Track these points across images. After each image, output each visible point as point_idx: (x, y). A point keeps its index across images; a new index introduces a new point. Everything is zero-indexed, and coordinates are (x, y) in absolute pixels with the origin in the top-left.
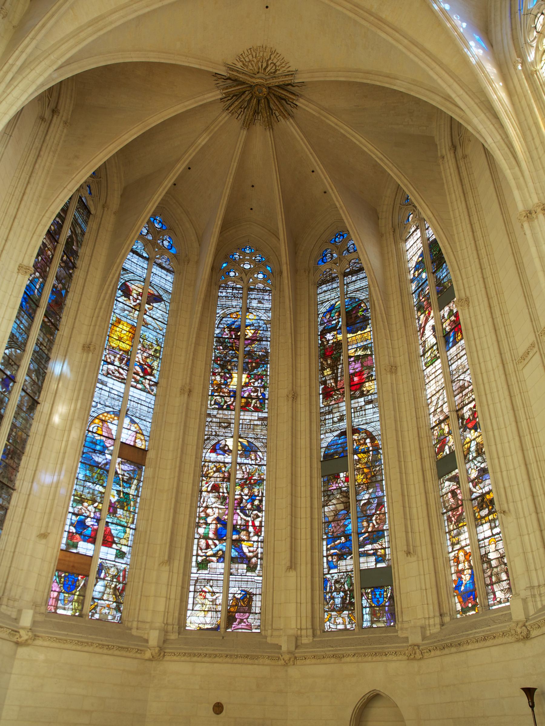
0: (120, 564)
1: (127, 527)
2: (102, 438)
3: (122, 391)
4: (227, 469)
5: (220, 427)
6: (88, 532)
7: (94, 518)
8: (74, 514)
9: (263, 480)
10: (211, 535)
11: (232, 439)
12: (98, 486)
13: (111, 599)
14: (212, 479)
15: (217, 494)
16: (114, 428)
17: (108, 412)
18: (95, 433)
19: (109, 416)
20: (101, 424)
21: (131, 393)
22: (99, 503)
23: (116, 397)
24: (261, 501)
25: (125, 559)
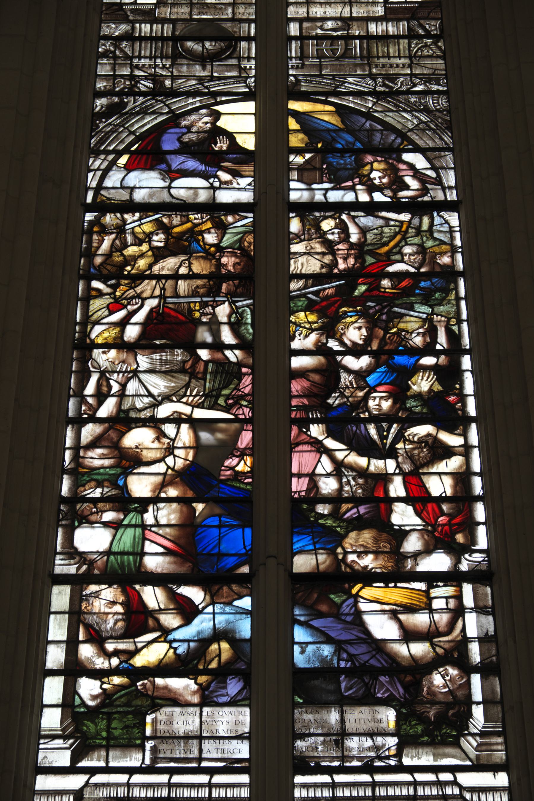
4: (228, 240)
5: (175, 57)
9: (450, 274)
10: (154, 563)
11: (250, 106)
14: (146, 287)
15: (179, 355)
24: (449, 375)
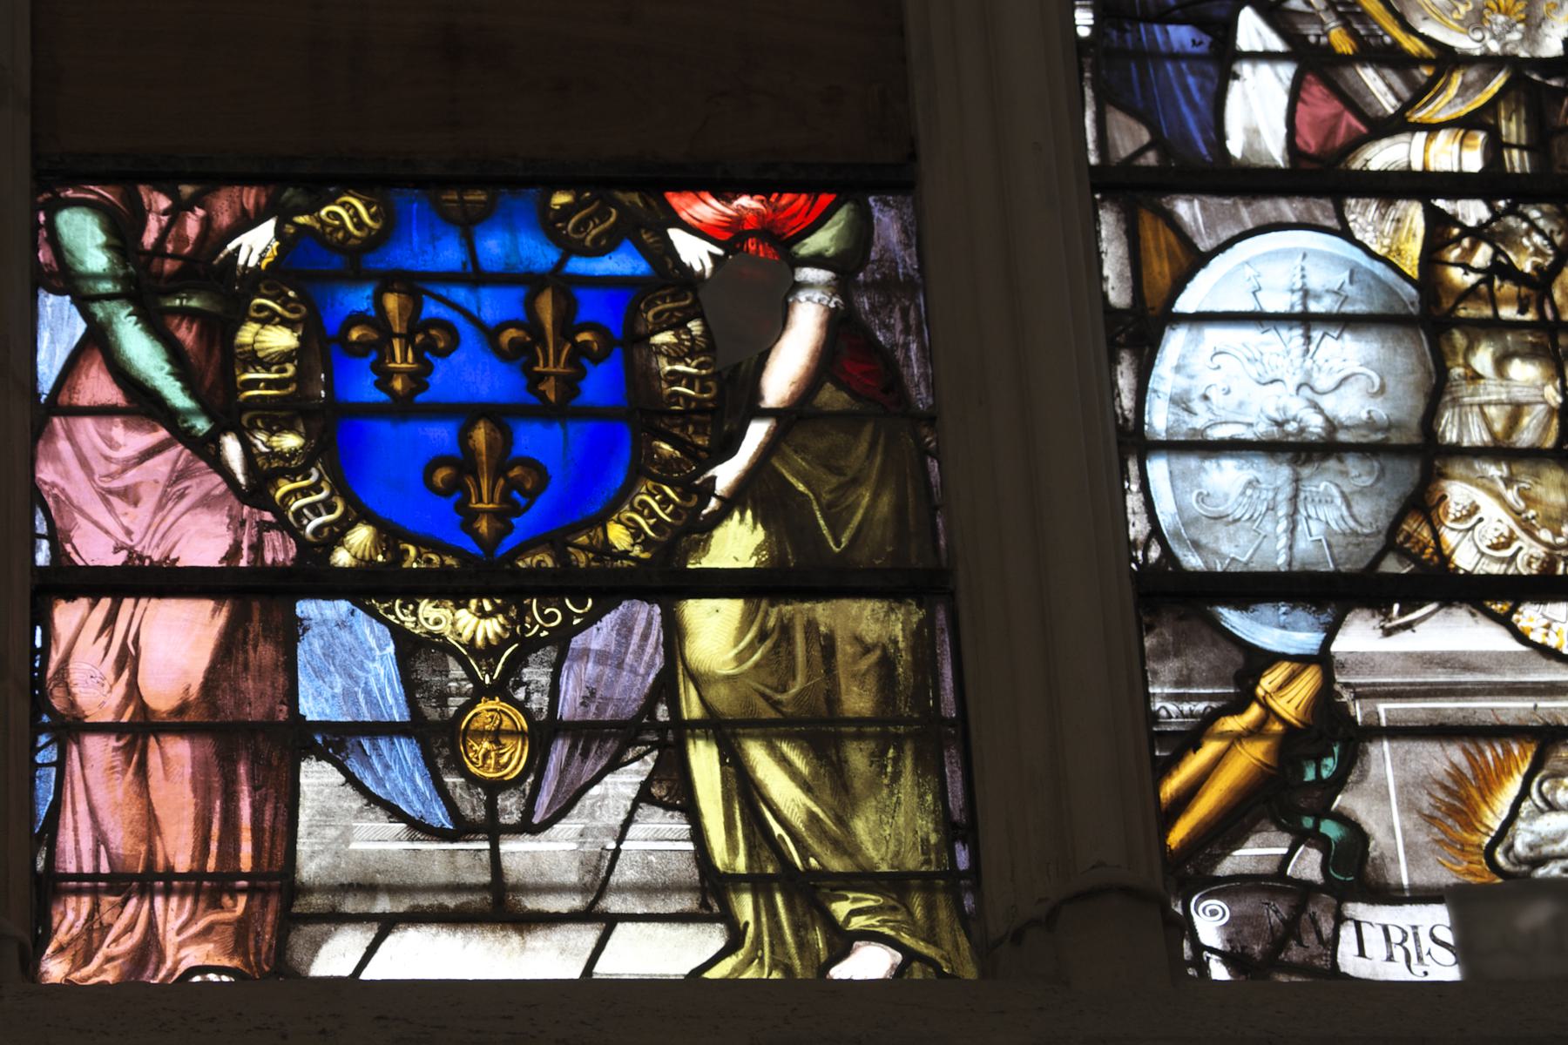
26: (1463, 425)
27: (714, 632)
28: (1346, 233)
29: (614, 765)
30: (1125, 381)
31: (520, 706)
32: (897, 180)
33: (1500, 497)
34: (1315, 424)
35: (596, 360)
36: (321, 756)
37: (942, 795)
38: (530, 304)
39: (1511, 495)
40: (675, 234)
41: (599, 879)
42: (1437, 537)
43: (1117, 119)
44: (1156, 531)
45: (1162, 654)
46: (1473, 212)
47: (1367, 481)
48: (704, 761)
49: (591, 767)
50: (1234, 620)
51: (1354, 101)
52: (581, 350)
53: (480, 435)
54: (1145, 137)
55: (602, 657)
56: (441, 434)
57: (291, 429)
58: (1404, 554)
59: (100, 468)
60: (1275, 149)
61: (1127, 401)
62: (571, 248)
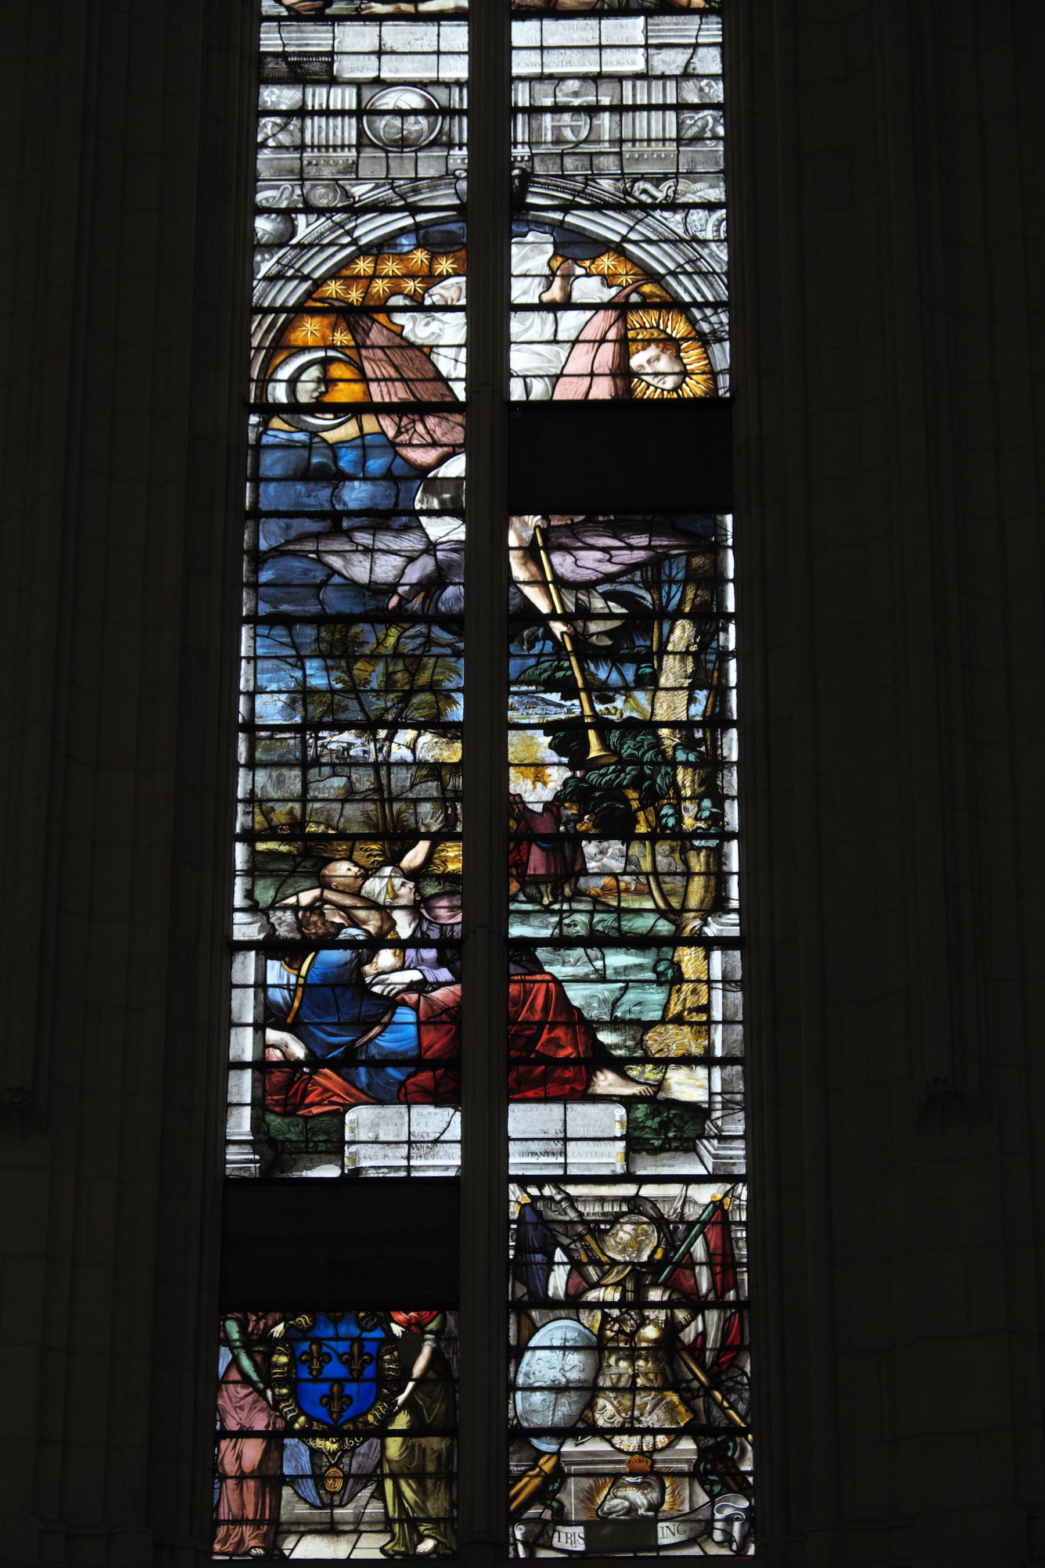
0: (674, 1190)
1: (677, 941)
2: (370, 424)
3: (458, 69)
6: (400, 1034)
7: (417, 942)
8: (270, 947)
12: (406, 735)
13: (651, 1420)
16: (445, 336)
17: (380, 248)
18: (318, 407)
19: (391, 267)
20: (342, 338)
21: (522, 64)
22: (436, 839)
23: (418, 126)
25: (708, 1147)
26: (605, 1381)
27: (394, 1447)
28: (578, 1321)
29: (365, 1487)
30: (512, 1369)
31: (341, 1469)
32: (454, 1307)
33: (612, 1403)
34: (564, 1380)
35: (369, 1363)
36: (288, 1485)
37: (451, 1496)
38: (351, 1347)
39: (615, 1403)
40: (393, 1325)
41: (358, 1520)
42: (593, 1416)
43: (518, 1285)
44: (516, 1415)
45: (514, 1453)
46: (615, 1313)
47: (576, 1399)
48: (389, 1485)
49: (359, 1487)
50: (535, 1442)
51: (585, 1277)
52: (365, 1361)
53: (335, 1388)
54: (525, 1290)
55: (364, 1455)
56: (325, 1388)
57: (284, 1387)
58: (584, 1421)
59: (234, 1400)
60: (561, 1293)
61: (512, 1375)
62: (364, 1329)
